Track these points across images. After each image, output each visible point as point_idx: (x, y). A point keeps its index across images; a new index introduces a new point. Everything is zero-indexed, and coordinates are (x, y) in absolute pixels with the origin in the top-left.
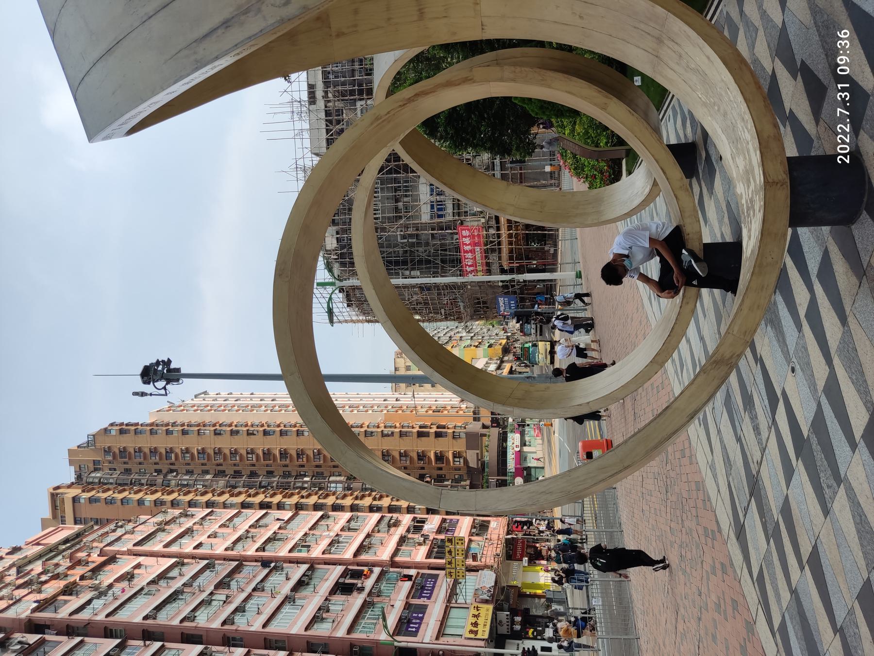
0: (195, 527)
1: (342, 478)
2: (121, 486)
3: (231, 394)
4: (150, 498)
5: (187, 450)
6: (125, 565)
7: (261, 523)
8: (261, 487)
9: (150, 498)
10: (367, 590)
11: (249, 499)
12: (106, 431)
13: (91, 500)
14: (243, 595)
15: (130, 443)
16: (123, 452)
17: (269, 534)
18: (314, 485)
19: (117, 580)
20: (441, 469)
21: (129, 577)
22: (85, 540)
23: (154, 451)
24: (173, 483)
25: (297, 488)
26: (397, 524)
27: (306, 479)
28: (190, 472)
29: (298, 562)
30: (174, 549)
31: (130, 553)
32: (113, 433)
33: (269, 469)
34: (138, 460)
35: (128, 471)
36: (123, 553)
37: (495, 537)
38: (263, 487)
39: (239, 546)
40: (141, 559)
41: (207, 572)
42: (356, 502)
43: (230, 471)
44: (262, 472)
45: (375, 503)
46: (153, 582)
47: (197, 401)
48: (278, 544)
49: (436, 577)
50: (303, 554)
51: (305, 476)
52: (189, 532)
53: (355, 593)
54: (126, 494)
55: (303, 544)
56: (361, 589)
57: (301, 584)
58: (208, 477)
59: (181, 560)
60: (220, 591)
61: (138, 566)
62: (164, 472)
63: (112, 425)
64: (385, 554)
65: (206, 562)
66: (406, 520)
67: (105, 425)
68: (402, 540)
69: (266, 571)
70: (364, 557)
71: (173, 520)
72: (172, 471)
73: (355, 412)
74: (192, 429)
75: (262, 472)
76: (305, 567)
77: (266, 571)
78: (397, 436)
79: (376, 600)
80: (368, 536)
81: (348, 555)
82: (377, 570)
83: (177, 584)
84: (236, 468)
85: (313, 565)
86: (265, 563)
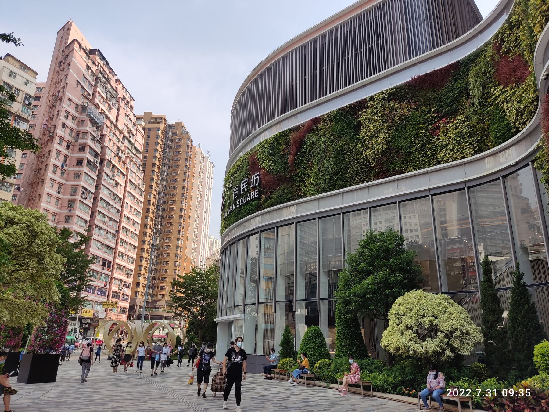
0: (136, 199)
1: (158, 242)
2: (165, 146)
3: (212, 178)
4: (156, 161)
5: (177, 174)
6: (121, 180)
7: (135, 223)
8: (157, 206)
9: (156, 161)
10: (103, 271)
11: (152, 203)
12: (189, 139)
13: (158, 136)
14: (105, 227)
15: (183, 149)
16: (179, 146)
17: (130, 228)
18: (156, 230)
19: (116, 181)
20: (158, 288)
21: (117, 184)
22: (134, 157)
23: (178, 160)
24: (164, 168)
25: (155, 222)
26: (128, 277)
27: (159, 226)
28: (168, 174)
29: (116, 244)
30: (127, 194)
31: (127, 179)
32: (188, 142)
33: (166, 210)
34: (175, 153)
35: (171, 147)
36: (127, 176)
37: (119, 317)
38: (157, 208)
39: (126, 219)
40: (124, 185)
41: (116, 210)
42: (146, 250)
43: (166, 192)
44: (165, 206)
45: (144, 259)
46: (114, 194)
47: (209, 164)
48: (125, 232)
49: (105, 296)
50: (119, 243)
51: (161, 225)
52: (134, 197)
53: (102, 267)
54: (160, 150)
55: (124, 242)
56: (103, 269)
57: (108, 247)
58: (165, 183)
59: (122, 200)
60: (108, 219)
61: (121, 185)
62: (169, 164)
63: (192, 141)
64: (117, 275)
65: (120, 209)
66: (130, 280)
67: (191, 138)
68: (121, 280)
69: (114, 232)
70: (116, 267)
71: (140, 189)
72: (169, 167)
73: (193, 244)
74: (187, 176)
75: (165, 206)
76: (113, 246)
77: (114, 232)
78: (175, 268)
79: (99, 275)
80: (124, 267)
81: (118, 261)
82: (110, 273)
83: (112, 203)
84: (167, 195)
85: (115, 249)
86: (117, 232)
